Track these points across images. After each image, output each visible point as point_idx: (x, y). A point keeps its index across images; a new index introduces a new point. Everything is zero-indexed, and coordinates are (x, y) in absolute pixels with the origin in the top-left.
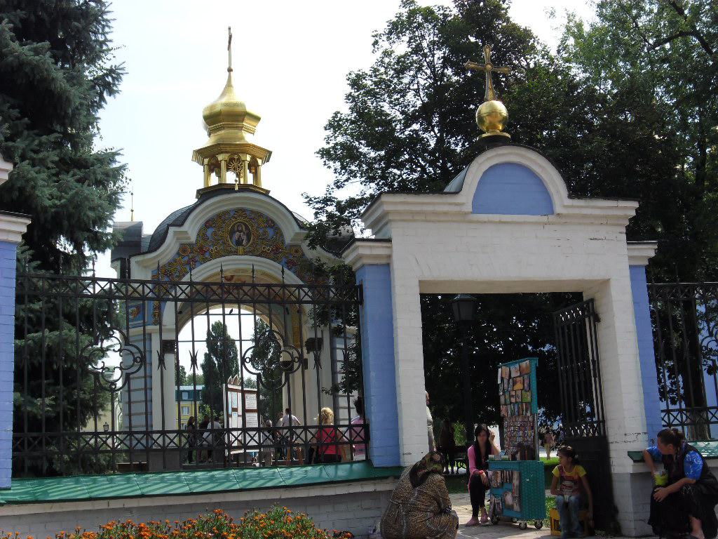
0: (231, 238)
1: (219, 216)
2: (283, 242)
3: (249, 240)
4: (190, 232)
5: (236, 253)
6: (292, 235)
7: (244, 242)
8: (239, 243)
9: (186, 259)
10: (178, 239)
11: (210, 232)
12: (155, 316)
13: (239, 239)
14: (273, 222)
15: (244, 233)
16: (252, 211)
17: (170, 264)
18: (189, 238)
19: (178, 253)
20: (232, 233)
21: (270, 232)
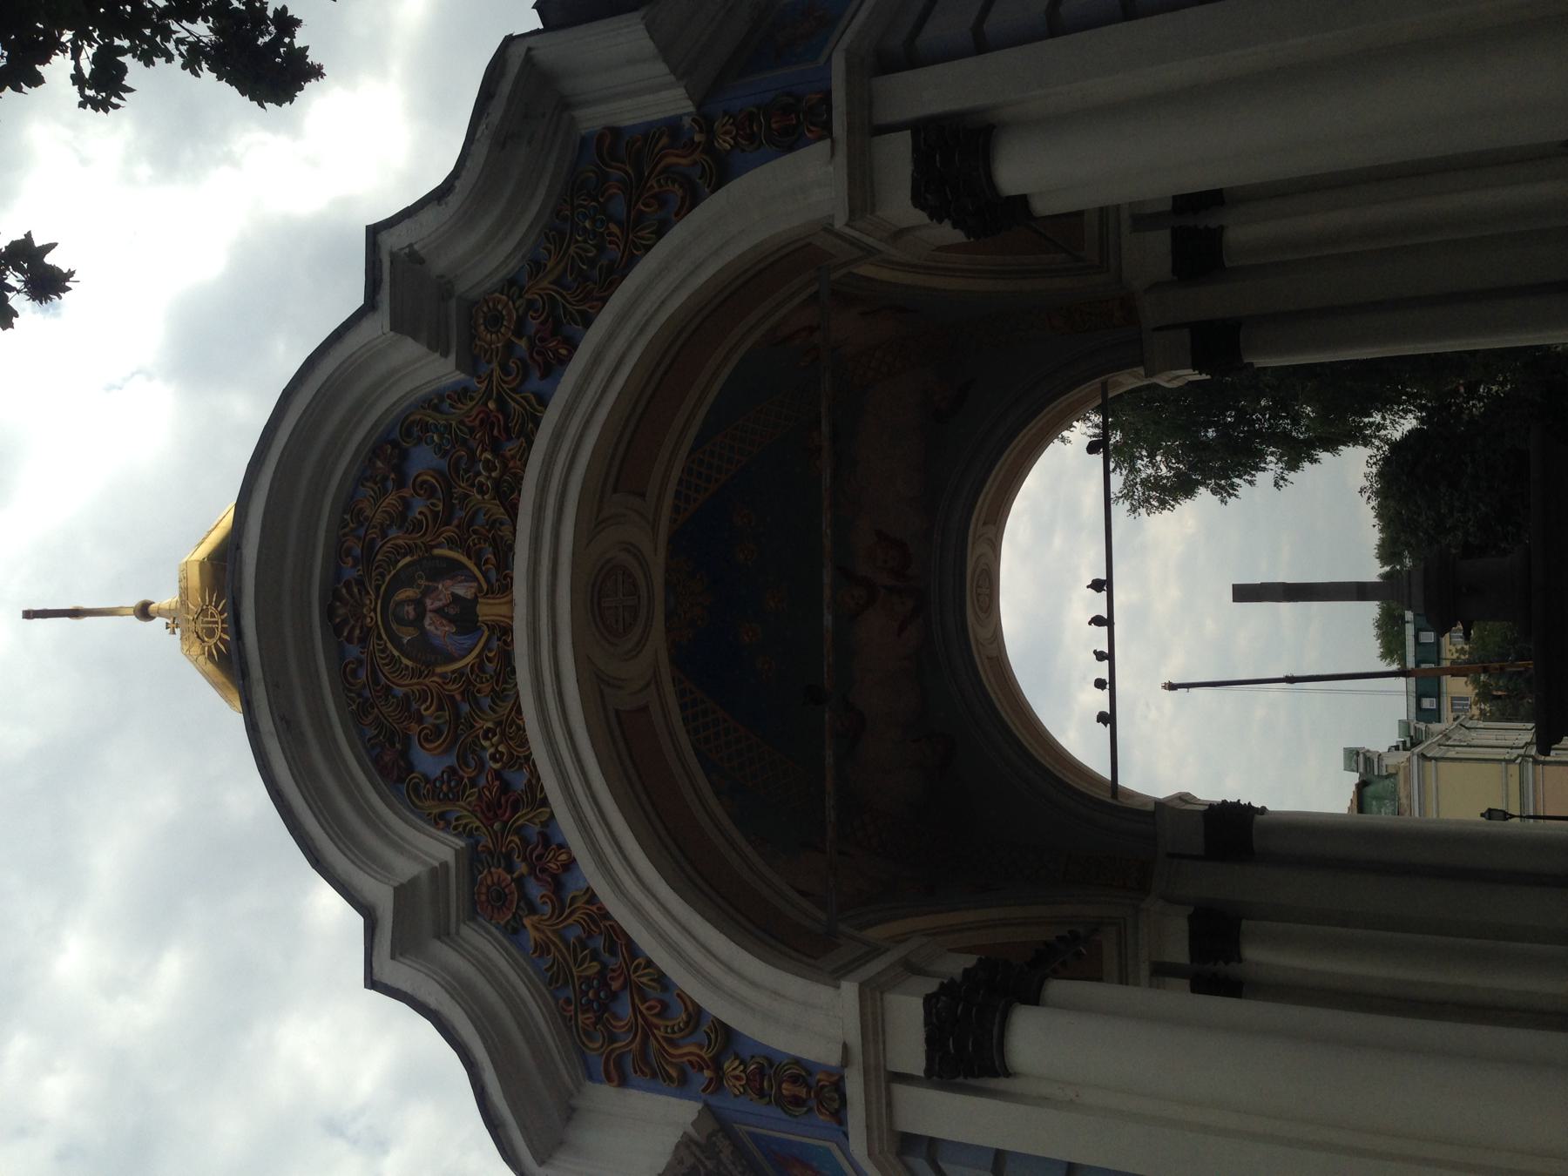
0: (452, 659)
2: (461, 394)
3: (452, 569)
4: (406, 869)
5: (505, 631)
6: (411, 348)
7: (464, 590)
8: (464, 617)
9: (536, 891)
10: (443, 933)
11: (429, 762)
12: (797, 1101)
13: (451, 620)
14: (376, 452)
15: (426, 592)
16: (338, 552)
17: (556, 979)
18: (438, 874)
19: (514, 931)
20: (428, 654)
21: (424, 460)
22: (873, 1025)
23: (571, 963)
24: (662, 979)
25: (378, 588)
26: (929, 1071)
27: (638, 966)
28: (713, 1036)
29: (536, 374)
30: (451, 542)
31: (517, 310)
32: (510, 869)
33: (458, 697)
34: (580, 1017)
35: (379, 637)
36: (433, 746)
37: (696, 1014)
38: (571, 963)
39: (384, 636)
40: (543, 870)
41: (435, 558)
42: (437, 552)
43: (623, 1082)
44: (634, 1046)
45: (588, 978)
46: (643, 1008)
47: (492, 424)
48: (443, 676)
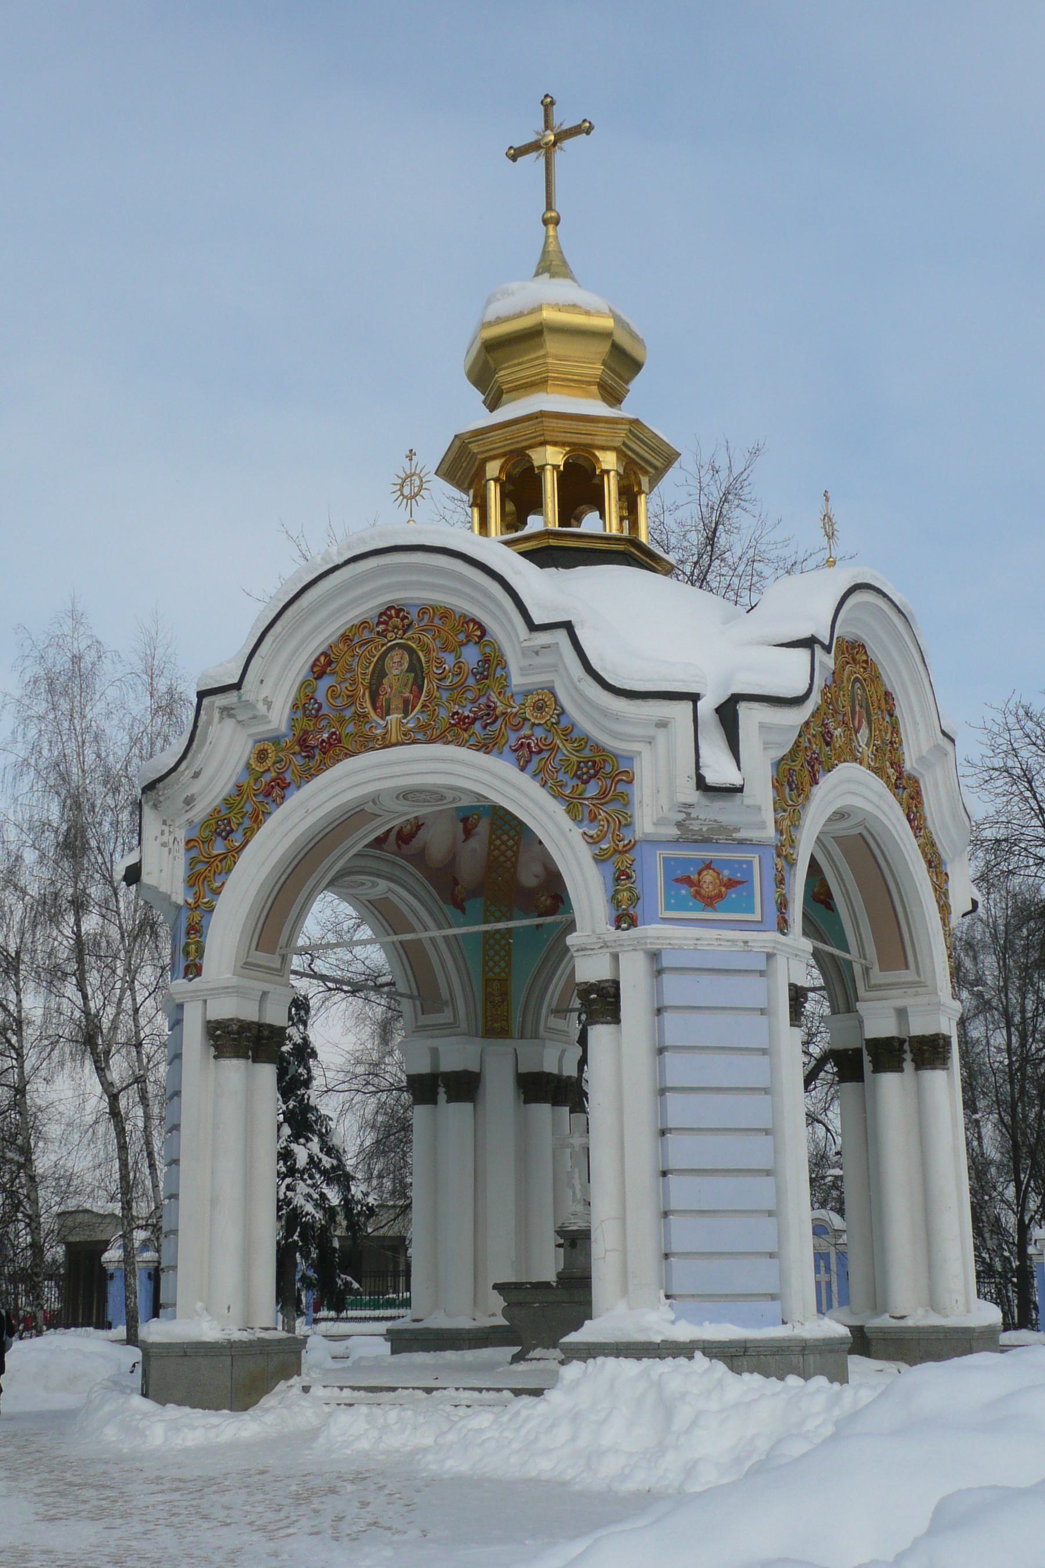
1: (345, 638)
18: (264, 719)
22: (225, 990)
23: (235, 812)
24: (229, 871)
25: (409, 639)
26: (209, 1022)
27: (234, 856)
28: (207, 905)
29: (513, 739)
30: (428, 692)
31: (546, 722)
32: (275, 763)
33: (353, 709)
34: (213, 821)
35: (383, 645)
36: (329, 695)
37: (217, 892)
38: (235, 812)
39: (385, 648)
40: (273, 787)
41: (423, 678)
42: (426, 681)
43: (188, 850)
44: (201, 857)
45: (229, 823)
46: (217, 862)
47: (488, 714)
48: (364, 694)
